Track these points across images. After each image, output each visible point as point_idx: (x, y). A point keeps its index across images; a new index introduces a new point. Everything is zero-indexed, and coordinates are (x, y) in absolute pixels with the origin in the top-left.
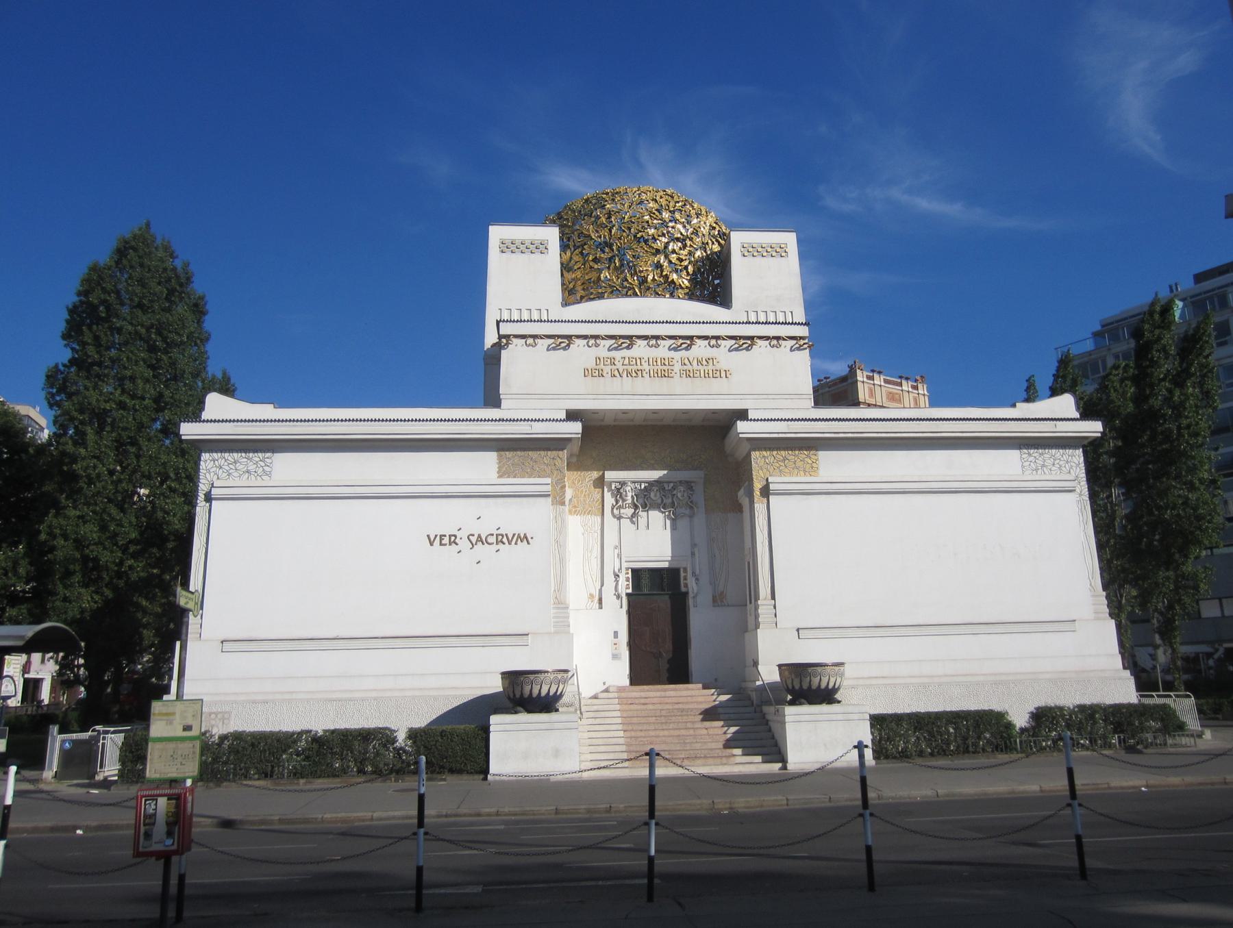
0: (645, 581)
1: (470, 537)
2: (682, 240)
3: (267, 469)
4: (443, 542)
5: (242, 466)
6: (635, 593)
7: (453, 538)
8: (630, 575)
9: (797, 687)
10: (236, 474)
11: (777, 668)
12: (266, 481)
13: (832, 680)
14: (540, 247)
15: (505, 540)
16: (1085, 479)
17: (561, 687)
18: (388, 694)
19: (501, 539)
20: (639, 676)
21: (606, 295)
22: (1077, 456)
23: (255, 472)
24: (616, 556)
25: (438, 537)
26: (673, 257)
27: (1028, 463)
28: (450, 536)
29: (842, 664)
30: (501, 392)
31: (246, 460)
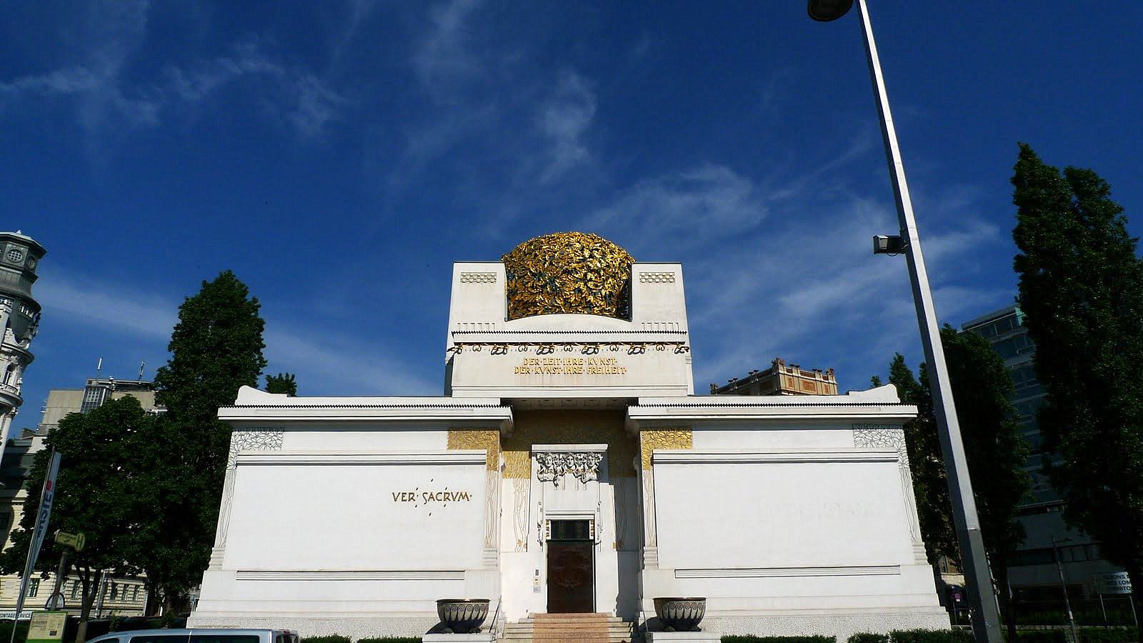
0: (561, 530)
2: (597, 271)
4: (404, 498)
5: (261, 440)
8: (550, 526)
10: (256, 446)
11: (653, 601)
13: (694, 612)
14: (491, 278)
15: (450, 497)
17: (481, 613)
18: (356, 616)
19: (447, 496)
20: (556, 605)
22: (900, 434)
25: (401, 495)
26: (590, 285)
27: (857, 439)
28: (410, 494)
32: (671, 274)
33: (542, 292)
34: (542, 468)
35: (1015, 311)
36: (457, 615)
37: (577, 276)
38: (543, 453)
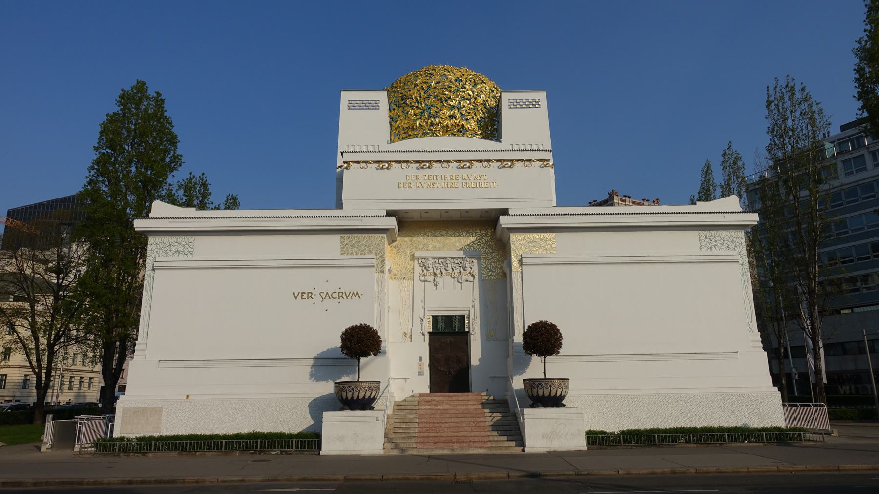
1: (321, 294)
3: (190, 250)
4: (303, 297)
6: (434, 331)
7: (310, 295)
8: (431, 320)
9: (535, 395)
10: (171, 253)
11: (523, 382)
12: (190, 257)
13: (559, 391)
15: (344, 296)
16: (746, 254)
19: (341, 295)
20: (436, 386)
21: (419, 135)
23: (183, 252)
24: (421, 307)
25: (300, 294)
27: (704, 243)
28: (308, 293)
29: (569, 379)
30: (343, 199)
31: (177, 244)
32: (537, 101)
33: (421, 118)
34: (423, 271)
35: (824, 145)
36: (352, 395)
37: (451, 103)
38: (425, 258)
